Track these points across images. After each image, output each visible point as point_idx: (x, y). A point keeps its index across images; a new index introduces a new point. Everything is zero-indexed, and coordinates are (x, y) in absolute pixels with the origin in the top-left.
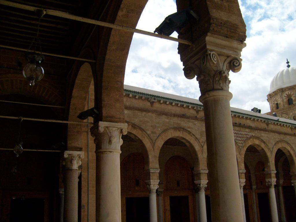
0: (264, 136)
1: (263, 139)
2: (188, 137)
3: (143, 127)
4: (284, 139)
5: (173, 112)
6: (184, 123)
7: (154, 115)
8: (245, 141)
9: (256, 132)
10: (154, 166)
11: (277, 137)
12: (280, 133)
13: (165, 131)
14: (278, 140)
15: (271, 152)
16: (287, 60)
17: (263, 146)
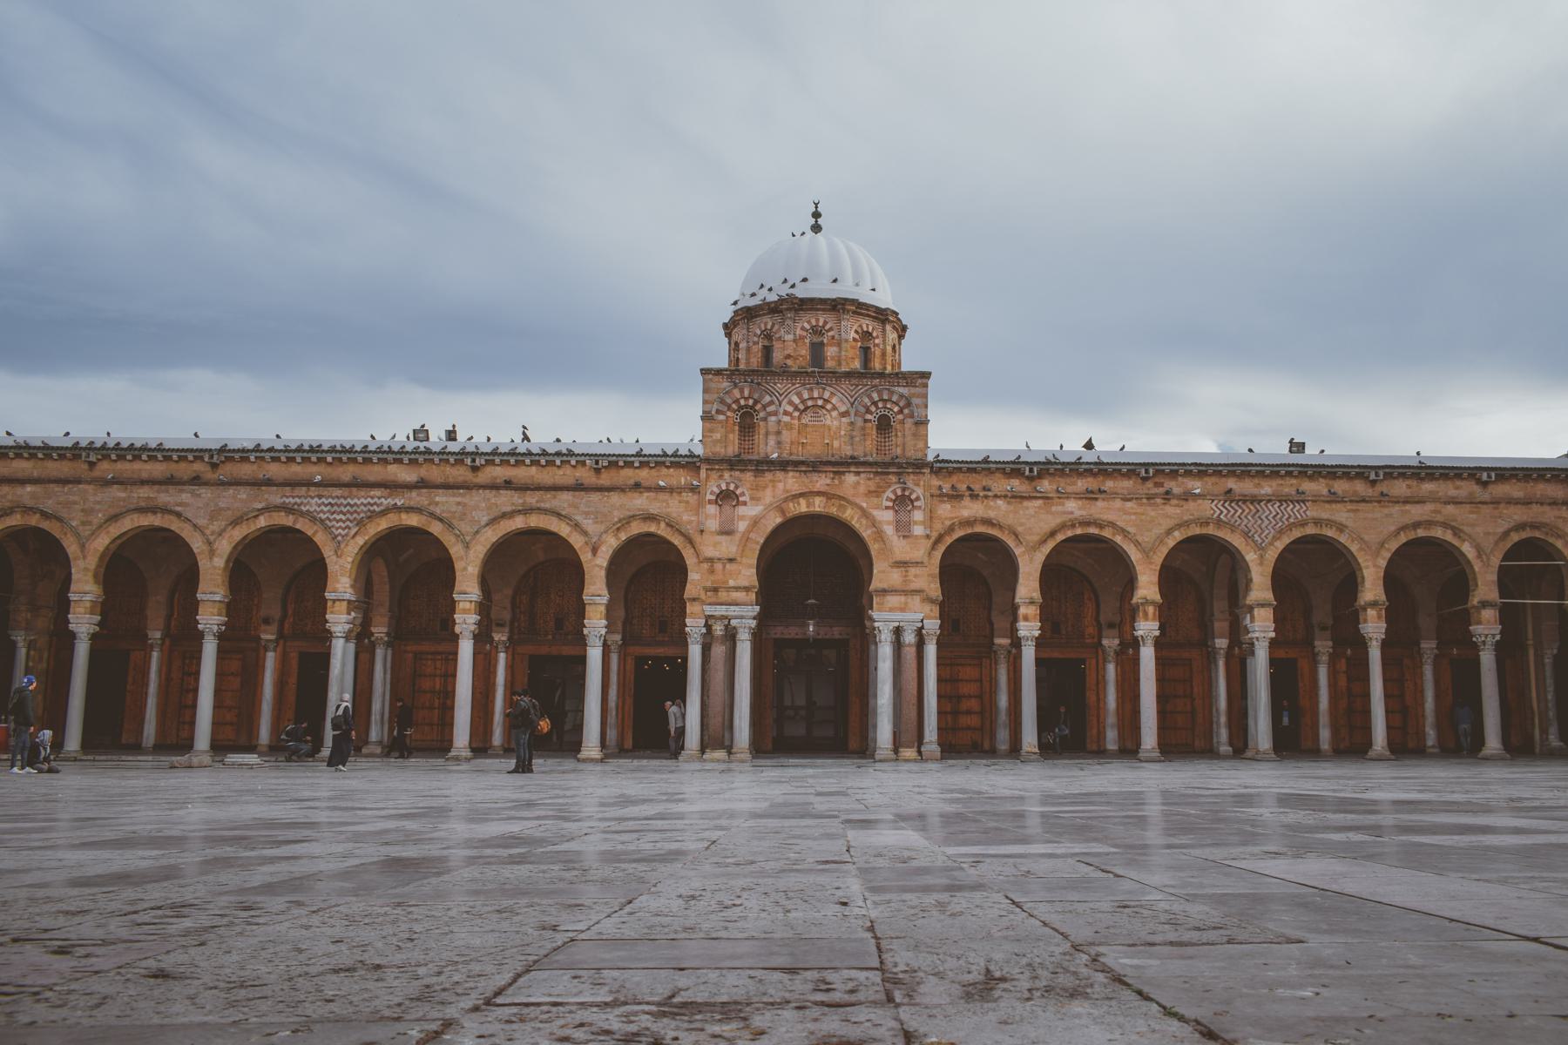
0: (445, 502)
1: (438, 511)
2: (175, 525)
3: (64, 514)
4: (547, 506)
5: (145, 475)
6: (165, 497)
7: (90, 488)
8: (360, 523)
9: (414, 494)
10: (85, 590)
11: (507, 500)
12: (524, 488)
13: (114, 518)
14: (509, 509)
15: (467, 546)
17: (436, 529)
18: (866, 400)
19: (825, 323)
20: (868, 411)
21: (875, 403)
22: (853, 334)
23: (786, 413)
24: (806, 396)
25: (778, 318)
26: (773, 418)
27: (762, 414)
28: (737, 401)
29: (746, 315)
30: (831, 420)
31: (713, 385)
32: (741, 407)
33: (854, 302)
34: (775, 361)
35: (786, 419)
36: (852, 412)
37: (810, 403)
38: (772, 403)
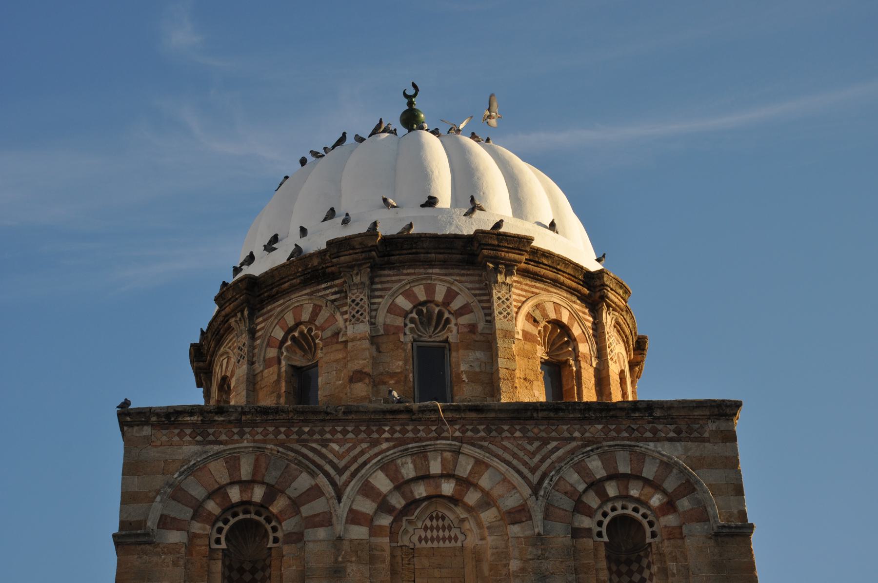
16: (411, 104)
18: (573, 478)
19: (451, 295)
20: (580, 507)
21: (597, 486)
22: (521, 324)
23: (355, 518)
24: (408, 470)
25: (327, 291)
26: (322, 533)
27: (288, 525)
28: (219, 492)
29: (247, 297)
30: (479, 534)
31: (152, 453)
32: (231, 509)
33: (522, 242)
34: (322, 394)
35: (359, 532)
36: (537, 510)
37: (420, 491)
38: (315, 492)
